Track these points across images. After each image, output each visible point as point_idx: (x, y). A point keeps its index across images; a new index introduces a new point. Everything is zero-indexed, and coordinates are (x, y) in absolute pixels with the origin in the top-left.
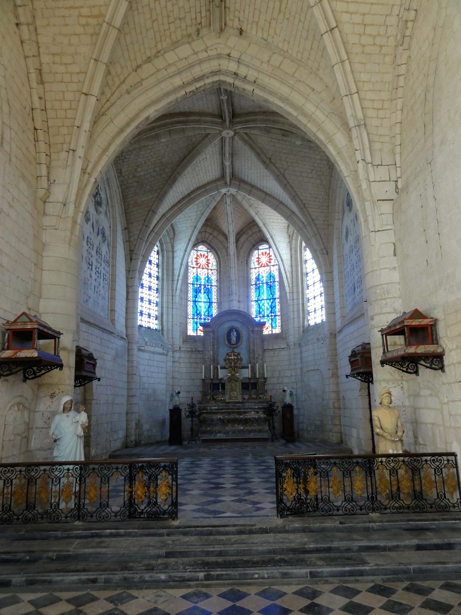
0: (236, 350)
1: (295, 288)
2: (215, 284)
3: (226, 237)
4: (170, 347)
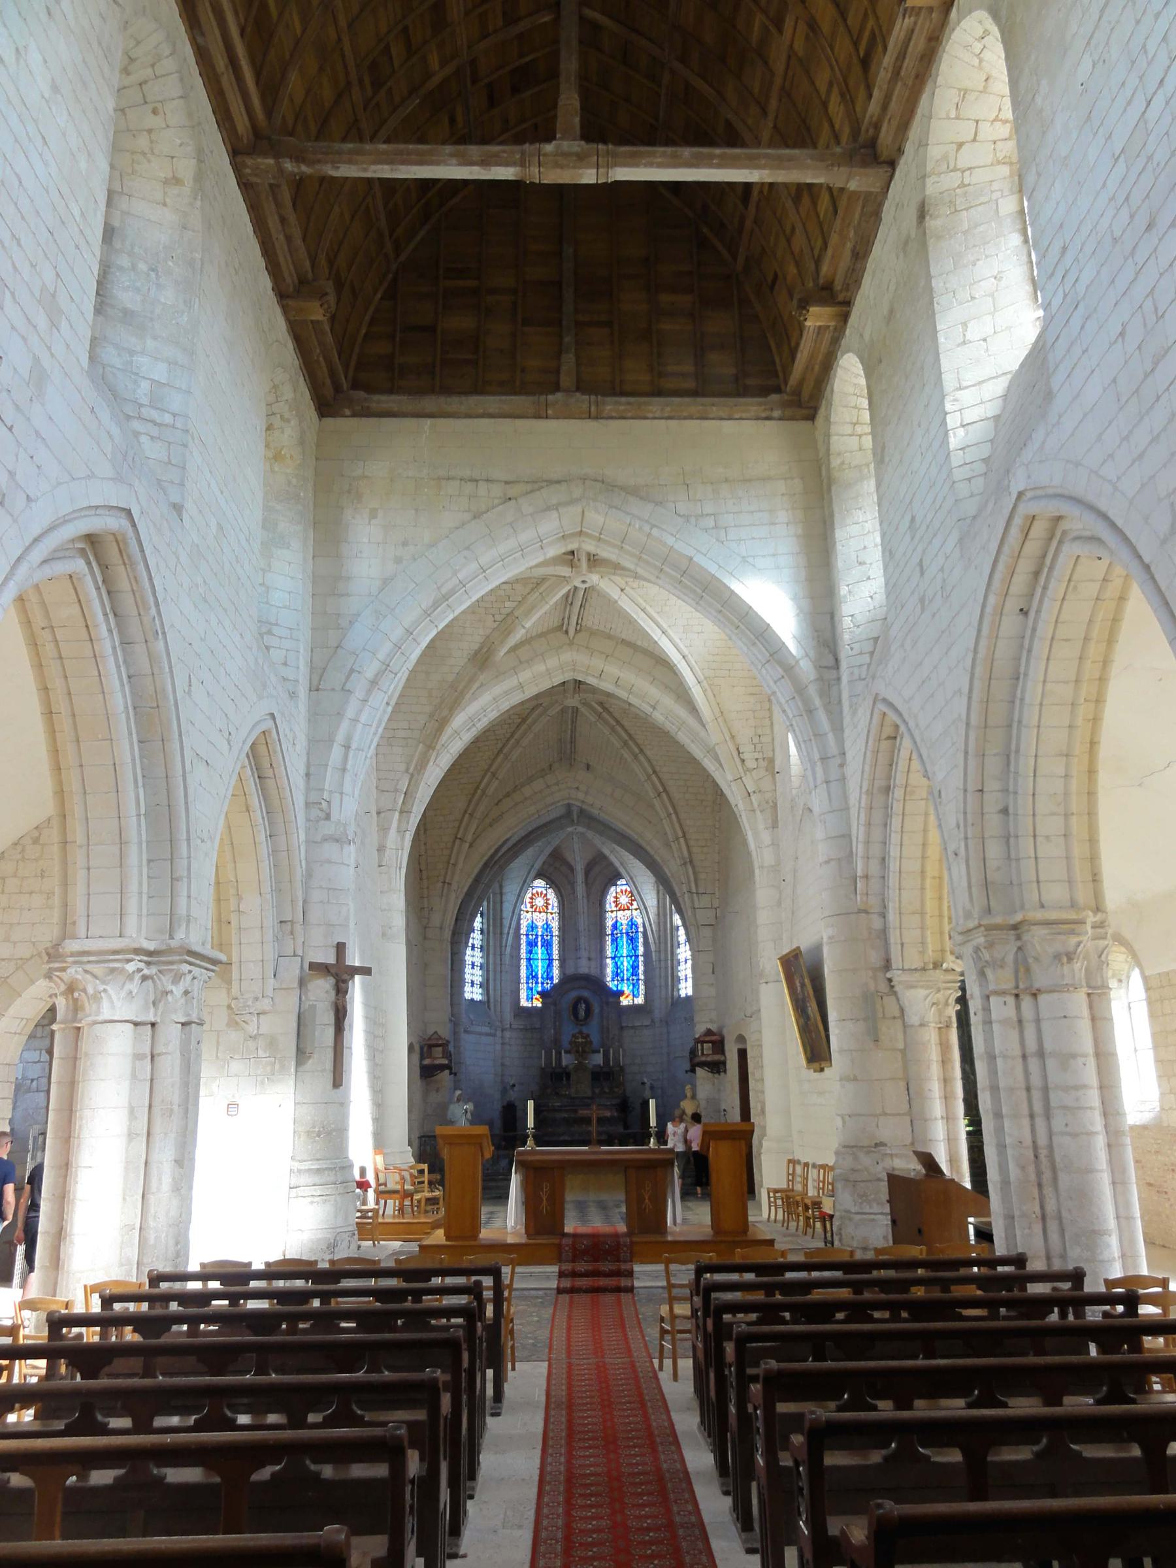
0: (585, 1030)
1: (662, 946)
2: (557, 933)
3: (572, 869)
4: (498, 1024)
